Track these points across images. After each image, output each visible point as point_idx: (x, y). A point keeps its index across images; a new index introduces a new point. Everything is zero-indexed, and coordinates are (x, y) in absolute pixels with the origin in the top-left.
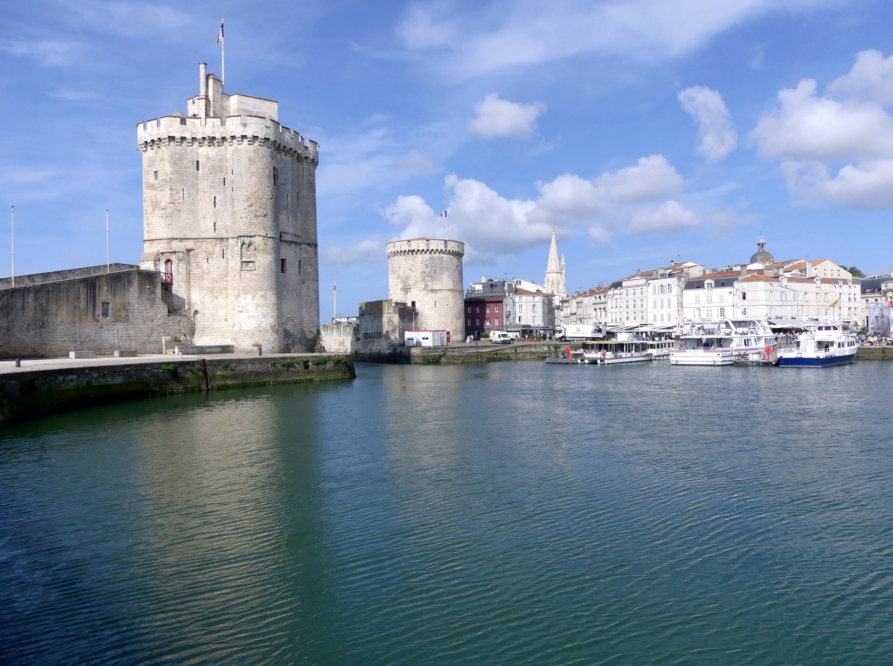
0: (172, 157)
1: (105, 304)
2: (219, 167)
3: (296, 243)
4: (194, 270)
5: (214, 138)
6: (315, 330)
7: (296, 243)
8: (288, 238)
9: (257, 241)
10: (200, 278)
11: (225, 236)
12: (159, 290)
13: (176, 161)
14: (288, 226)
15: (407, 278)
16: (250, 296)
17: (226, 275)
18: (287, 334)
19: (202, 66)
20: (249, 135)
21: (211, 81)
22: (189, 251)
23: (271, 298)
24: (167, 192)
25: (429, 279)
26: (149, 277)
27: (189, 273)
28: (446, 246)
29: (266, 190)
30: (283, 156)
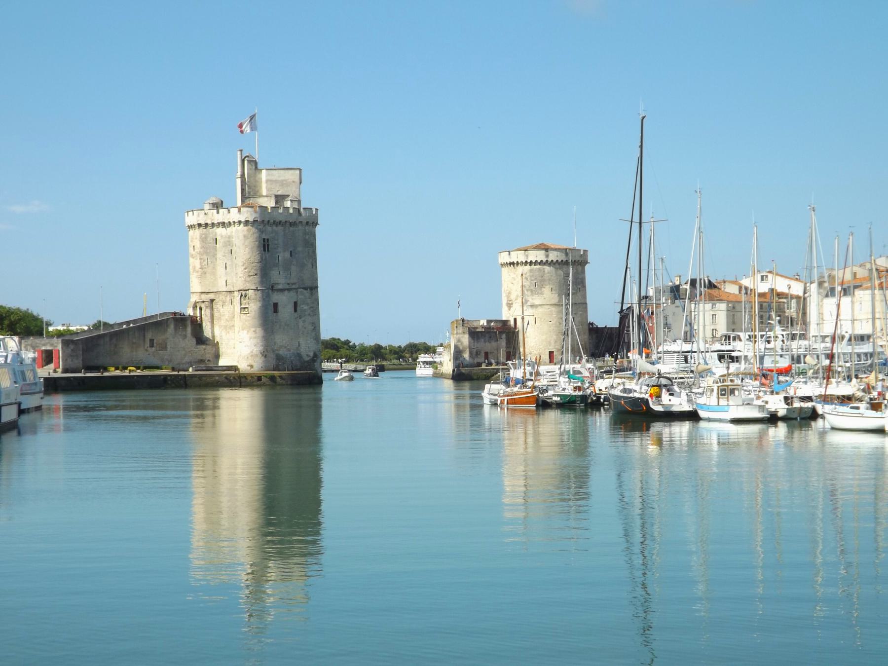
0: (201, 235)
1: (152, 341)
2: (229, 242)
3: (288, 289)
4: (216, 314)
5: (224, 223)
6: (311, 354)
7: (288, 289)
8: (280, 287)
9: (250, 293)
10: (219, 319)
11: (232, 289)
12: (189, 329)
13: (203, 239)
14: (278, 278)
15: (509, 293)
16: (245, 332)
17: (234, 317)
18: (279, 358)
19: (239, 153)
20: (243, 220)
21: (246, 162)
22: (212, 301)
23: (260, 332)
24: (198, 261)
25: (529, 293)
26: (180, 320)
27: (212, 316)
28: (547, 256)
29: (256, 257)
30: (274, 228)
